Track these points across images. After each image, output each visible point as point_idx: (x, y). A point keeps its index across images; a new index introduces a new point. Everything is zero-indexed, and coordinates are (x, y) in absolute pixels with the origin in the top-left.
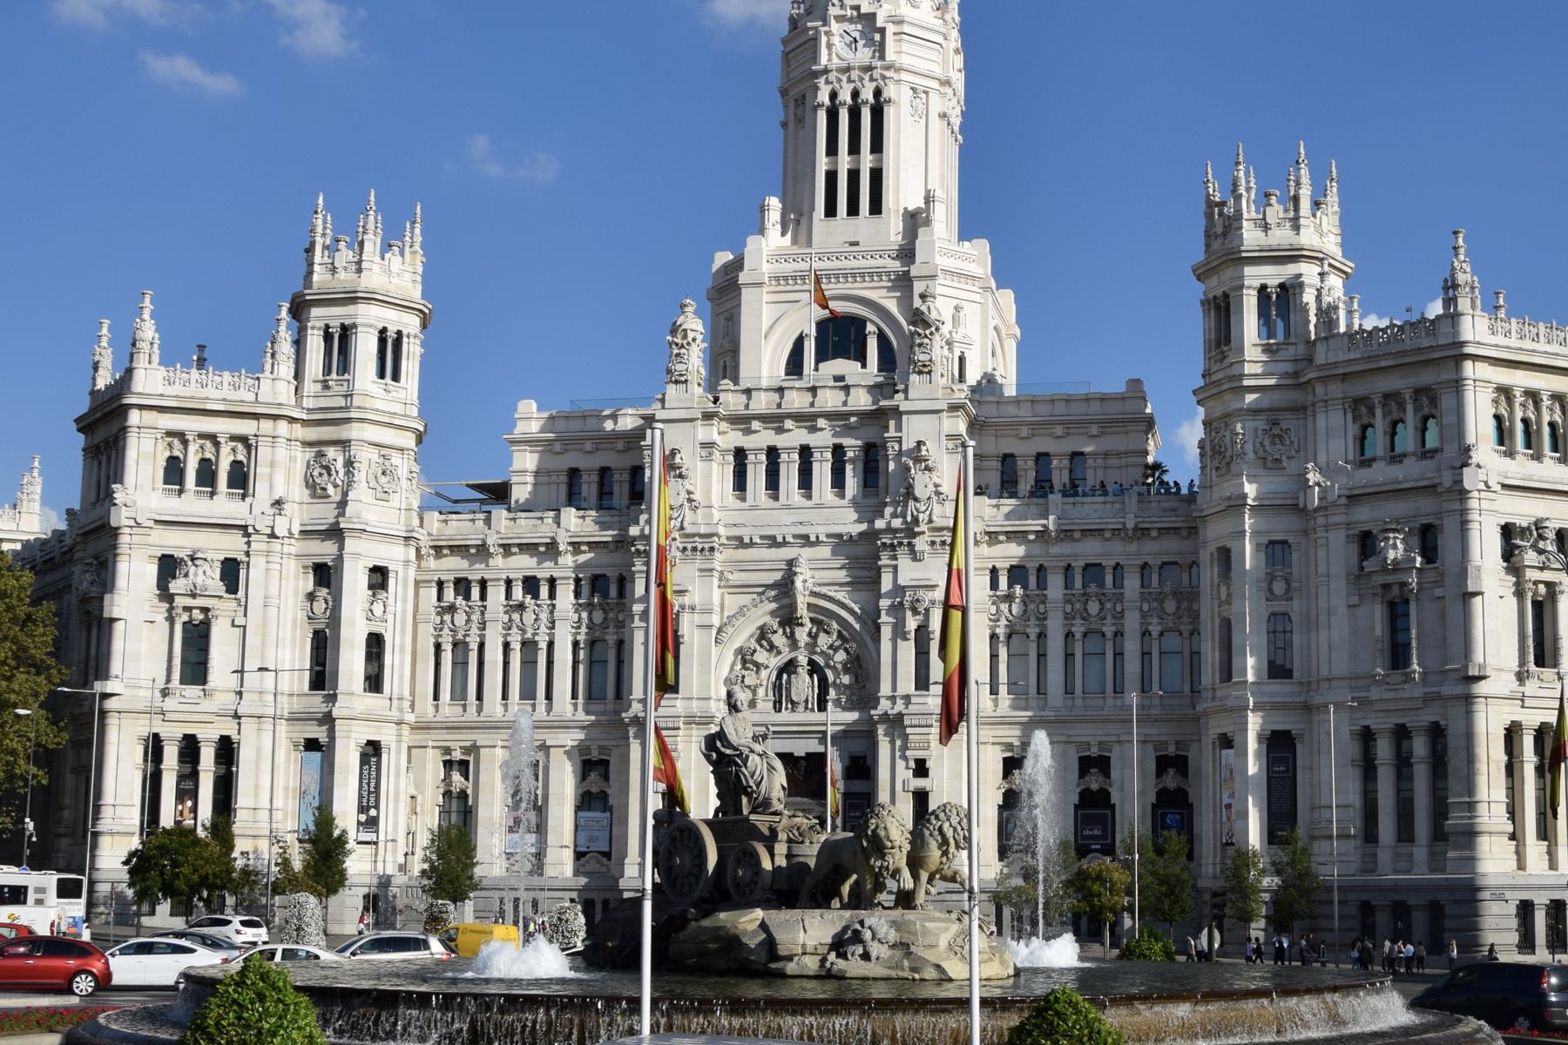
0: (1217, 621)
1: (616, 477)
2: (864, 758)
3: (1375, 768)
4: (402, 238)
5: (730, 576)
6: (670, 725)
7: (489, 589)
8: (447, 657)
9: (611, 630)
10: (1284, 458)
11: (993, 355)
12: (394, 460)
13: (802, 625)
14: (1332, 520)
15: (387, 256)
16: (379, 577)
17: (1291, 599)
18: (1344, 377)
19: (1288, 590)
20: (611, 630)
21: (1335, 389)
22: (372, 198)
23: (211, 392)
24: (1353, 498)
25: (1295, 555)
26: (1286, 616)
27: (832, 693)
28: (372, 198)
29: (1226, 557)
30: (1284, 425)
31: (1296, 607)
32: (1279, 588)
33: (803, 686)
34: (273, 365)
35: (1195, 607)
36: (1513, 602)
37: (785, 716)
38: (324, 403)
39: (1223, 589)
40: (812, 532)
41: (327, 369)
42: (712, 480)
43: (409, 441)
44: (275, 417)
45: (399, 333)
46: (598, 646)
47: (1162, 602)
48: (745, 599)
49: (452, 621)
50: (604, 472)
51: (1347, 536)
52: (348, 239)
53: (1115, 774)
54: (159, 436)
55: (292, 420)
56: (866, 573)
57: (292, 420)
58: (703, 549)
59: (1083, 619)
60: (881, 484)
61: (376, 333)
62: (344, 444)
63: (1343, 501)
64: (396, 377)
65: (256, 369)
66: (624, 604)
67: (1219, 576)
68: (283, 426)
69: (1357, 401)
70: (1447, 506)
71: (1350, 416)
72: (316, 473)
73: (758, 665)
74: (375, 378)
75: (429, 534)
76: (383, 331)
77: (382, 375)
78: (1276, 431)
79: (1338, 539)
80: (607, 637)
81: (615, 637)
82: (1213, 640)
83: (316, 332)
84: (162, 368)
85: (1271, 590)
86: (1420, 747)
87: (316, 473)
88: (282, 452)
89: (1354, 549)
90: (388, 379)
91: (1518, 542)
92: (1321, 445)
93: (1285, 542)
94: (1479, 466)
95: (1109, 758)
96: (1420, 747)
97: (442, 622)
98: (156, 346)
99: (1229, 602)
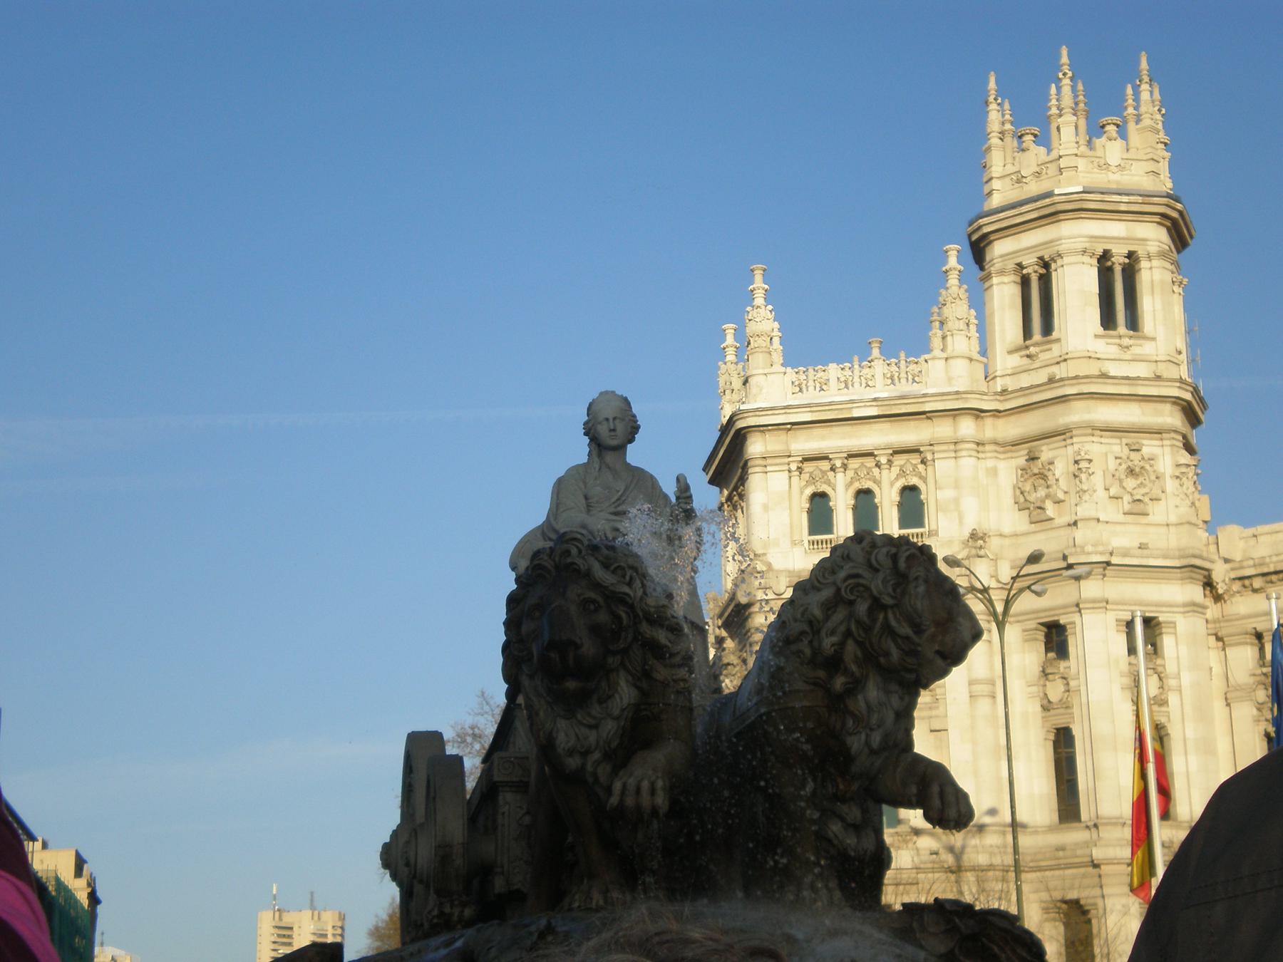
4: (1119, 109)
15: (1098, 142)
22: (1065, 59)
23: (857, 392)
28: (1065, 59)
34: (944, 338)
38: (1025, 380)
41: (1027, 333)
43: (1172, 418)
44: (955, 413)
45: (1130, 255)
52: (1036, 130)
54: (794, 467)
55: (978, 413)
57: (978, 413)
61: (1095, 262)
62: (1062, 434)
64: (1133, 323)
65: (920, 347)
68: (967, 427)
72: (1028, 487)
74: (1100, 330)
76: (1105, 257)
77: (1108, 320)
83: (1006, 279)
84: (789, 370)
87: (1028, 487)
90: (1122, 329)
98: (776, 341)
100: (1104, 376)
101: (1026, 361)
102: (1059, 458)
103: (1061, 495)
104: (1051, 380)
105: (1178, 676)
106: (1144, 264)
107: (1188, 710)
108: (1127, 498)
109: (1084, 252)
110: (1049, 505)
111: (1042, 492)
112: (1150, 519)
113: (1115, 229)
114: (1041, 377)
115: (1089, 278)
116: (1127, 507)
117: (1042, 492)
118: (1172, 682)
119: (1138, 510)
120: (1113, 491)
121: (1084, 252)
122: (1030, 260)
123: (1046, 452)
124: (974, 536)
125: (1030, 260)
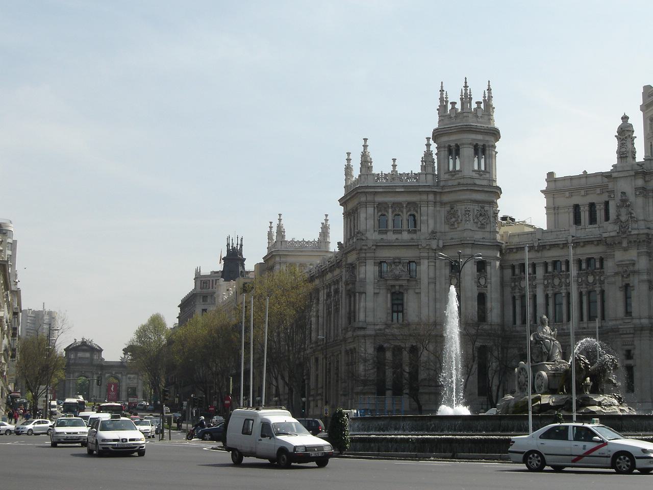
1: (598, 207)
6: (628, 332)
8: (518, 302)
9: (598, 285)
12: (486, 208)
16: (481, 266)
20: (598, 285)
38: (450, 183)
44: (427, 193)
45: (484, 145)
46: (592, 294)
50: (592, 206)
55: (435, 193)
66: (603, 272)
80: (596, 289)
88: (431, 208)
97: (515, 286)
100: (475, 184)
102: (460, 209)
104: (459, 184)
106: (487, 149)
109: (470, 144)
111: (454, 219)
112: (486, 230)
113: (480, 137)
114: (455, 183)
116: (479, 226)
117: (454, 219)
119: (482, 226)
121: (470, 144)
122: (453, 144)
125: (453, 144)
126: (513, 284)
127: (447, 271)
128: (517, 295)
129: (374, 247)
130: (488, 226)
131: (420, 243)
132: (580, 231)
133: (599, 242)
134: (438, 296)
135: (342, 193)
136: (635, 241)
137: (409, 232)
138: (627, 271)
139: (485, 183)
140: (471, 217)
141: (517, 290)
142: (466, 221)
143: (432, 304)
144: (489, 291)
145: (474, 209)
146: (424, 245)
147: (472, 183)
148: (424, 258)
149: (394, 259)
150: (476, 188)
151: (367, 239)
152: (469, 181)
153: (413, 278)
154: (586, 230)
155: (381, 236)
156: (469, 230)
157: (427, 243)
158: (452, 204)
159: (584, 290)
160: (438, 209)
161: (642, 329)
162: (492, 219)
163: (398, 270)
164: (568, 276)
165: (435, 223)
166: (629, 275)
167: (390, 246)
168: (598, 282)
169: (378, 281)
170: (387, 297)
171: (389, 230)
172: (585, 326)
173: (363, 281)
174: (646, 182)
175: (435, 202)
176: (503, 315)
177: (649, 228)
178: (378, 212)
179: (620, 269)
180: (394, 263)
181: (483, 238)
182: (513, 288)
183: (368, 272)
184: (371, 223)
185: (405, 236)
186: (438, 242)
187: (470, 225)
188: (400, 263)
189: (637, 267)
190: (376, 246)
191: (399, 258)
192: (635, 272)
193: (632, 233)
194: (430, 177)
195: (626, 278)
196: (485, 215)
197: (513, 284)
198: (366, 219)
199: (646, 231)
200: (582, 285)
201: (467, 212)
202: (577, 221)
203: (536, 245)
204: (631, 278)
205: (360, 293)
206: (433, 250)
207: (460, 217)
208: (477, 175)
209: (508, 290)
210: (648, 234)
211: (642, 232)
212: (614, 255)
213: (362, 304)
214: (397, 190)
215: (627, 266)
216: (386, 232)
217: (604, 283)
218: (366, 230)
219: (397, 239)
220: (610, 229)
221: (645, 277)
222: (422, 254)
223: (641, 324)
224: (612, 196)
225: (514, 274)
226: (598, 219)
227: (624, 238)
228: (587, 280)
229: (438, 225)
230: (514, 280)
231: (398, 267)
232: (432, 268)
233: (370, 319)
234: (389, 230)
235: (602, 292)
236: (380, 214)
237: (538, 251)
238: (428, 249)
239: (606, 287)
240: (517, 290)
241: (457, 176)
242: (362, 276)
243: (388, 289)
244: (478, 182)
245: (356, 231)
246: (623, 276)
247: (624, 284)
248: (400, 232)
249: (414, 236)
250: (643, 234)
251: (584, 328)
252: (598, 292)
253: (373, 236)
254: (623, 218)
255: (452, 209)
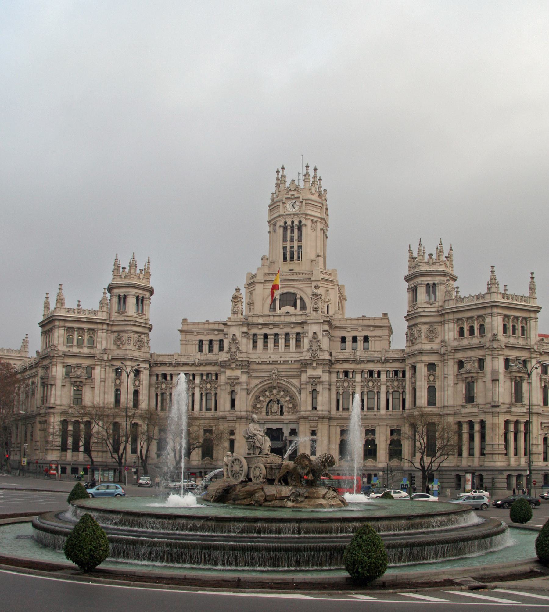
0: (411, 389)
2: (295, 430)
3: (462, 434)
5: (252, 374)
7: (173, 377)
8: (159, 398)
9: (213, 389)
10: (434, 338)
11: (338, 305)
13: (275, 389)
14: (450, 357)
17: (435, 382)
18: (454, 312)
19: (434, 379)
21: (451, 316)
24: (457, 350)
25: (437, 368)
26: (434, 387)
27: (285, 409)
29: (414, 368)
30: (435, 327)
31: (437, 385)
32: (432, 378)
33: (275, 407)
35: (404, 384)
36: (508, 383)
37: (270, 417)
38: (118, 319)
39: (413, 379)
40: (279, 360)
42: (245, 344)
47: (393, 382)
48: (257, 381)
49: (161, 387)
51: (454, 362)
53: (377, 435)
56: (296, 373)
58: (243, 365)
59: (367, 387)
60: (302, 345)
63: (453, 351)
67: (412, 374)
68: (105, 327)
69: (458, 320)
70: (487, 353)
71: (456, 325)
72: (117, 341)
73: (260, 401)
75: (154, 360)
78: (431, 329)
79: (451, 363)
81: (214, 392)
82: (409, 394)
85: (429, 379)
86: (477, 427)
89: (456, 367)
91: (511, 364)
92: (446, 334)
93: (434, 364)
94: (498, 340)
95: (375, 430)
96: (477, 427)
97: (158, 387)
99: (415, 383)
101: (119, 315)
102: (125, 336)
103: (124, 343)
105: (143, 382)
107: (144, 388)
108: (137, 346)
110: (121, 345)
115: (134, 300)
116: (137, 347)
118: (141, 382)
119: (139, 349)
120: (135, 344)
123: (122, 334)
124: (105, 349)
126: (157, 386)
127: (113, 375)
128: (159, 393)
129: (63, 356)
130: (143, 348)
131: (96, 355)
132: (203, 356)
133: (216, 364)
134: (106, 390)
135: (41, 319)
136: (240, 365)
137: (88, 347)
138: (233, 383)
139: (142, 321)
140: (132, 342)
141: (159, 390)
142: (128, 344)
143: (102, 395)
144: (141, 389)
145: (134, 337)
146: (98, 357)
147: (134, 320)
148: (98, 365)
149: (78, 364)
150: (137, 324)
151: (58, 350)
152: (132, 319)
153: (90, 377)
154: (208, 356)
155: (69, 349)
156: (130, 350)
157: (102, 356)
158: (119, 332)
159: (204, 393)
160: (109, 334)
161: (241, 418)
162: (145, 344)
163: (79, 372)
164: (194, 383)
165: (107, 343)
166: (235, 385)
167: (74, 356)
168: (213, 388)
169: (65, 378)
170: (71, 389)
171: (74, 346)
172: (203, 414)
173: (54, 377)
174: (249, 329)
175: (108, 330)
176: (149, 405)
177: (249, 358)
178: (67, 333)
179: (229, 381)
180: (77, 367)
181: (139, 356)
182: (156, 388)
183: (58, 371)
184: (61, 340)
185: (85, 350)
186: (108, 356)
187: (131, 347)
188: (81, 367)
189: (240, 380)
190: (65, 355)
191: (81, 364)
192: (240, 384)
193: (238, 360)
194: (105, 314)
195: (233, 386)
196: (141, 341)
197: (157, 386)
198: (58, 337)
199: (247, 359)
200: (203, 389)
201: (129, 338)
202: (201, 349)
203: (174, 362)
204: (236, 387)
205: (52, 385)
206: (104, 360)
207: (124, 341)
208: (137, 316)
209: (153, 390)
210: (248, 361)
211: (244, 359)
212: (225, 372)
213: (53, 392)
214: (82, 320)
215: (234, 379)
216: (72, 346)
217: (217, 389)
218: (58, 344)
219: (80, 351)
220: (224, 357)
221: (245, 387)
222: (97, 363)
223: (241, 414)
224: (227, 336)
225: (157, 379)
226: (214, 350)
227: (233, 362)
228: (206, 387)
229: (109, 345)
230: (157, 384)
231: (80, 370)
232: (103, 372)
233: (58, 402)
234: (74, 346)
235: (216, 394)
236: (68, 334)
237: (175, 367)
238: (101, 360)
239: (218, 391)
240: (159, 390)
241: (124, 315)
242: (54, 374)
243: (72, 384)
244: (138, 320)
245: (51, 344)
246: (231, 385)
247: (231, 390)
248: (82, 347)
249: (92, 351)
250: (245, 361)
251: (203, 415)
252: (213, 394)
253: (62, 348)
254: (233, 350)
255: (119, 335)
